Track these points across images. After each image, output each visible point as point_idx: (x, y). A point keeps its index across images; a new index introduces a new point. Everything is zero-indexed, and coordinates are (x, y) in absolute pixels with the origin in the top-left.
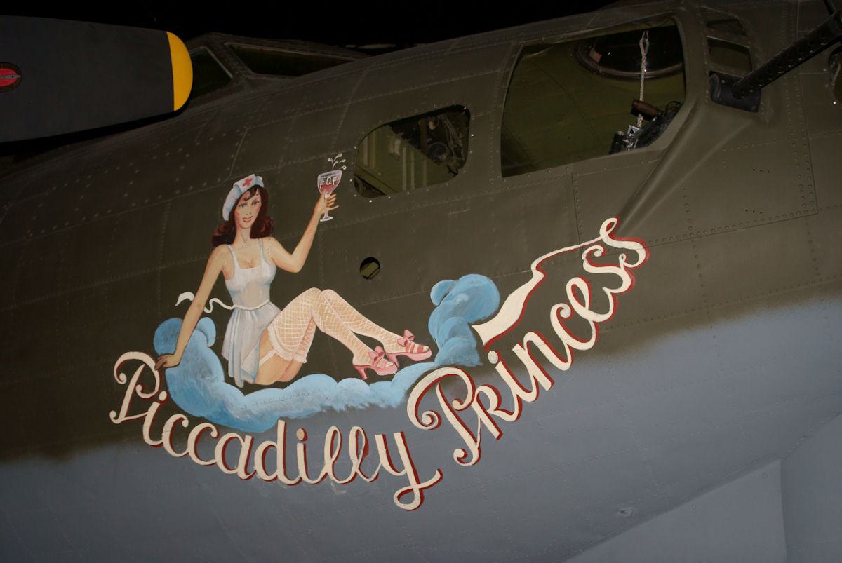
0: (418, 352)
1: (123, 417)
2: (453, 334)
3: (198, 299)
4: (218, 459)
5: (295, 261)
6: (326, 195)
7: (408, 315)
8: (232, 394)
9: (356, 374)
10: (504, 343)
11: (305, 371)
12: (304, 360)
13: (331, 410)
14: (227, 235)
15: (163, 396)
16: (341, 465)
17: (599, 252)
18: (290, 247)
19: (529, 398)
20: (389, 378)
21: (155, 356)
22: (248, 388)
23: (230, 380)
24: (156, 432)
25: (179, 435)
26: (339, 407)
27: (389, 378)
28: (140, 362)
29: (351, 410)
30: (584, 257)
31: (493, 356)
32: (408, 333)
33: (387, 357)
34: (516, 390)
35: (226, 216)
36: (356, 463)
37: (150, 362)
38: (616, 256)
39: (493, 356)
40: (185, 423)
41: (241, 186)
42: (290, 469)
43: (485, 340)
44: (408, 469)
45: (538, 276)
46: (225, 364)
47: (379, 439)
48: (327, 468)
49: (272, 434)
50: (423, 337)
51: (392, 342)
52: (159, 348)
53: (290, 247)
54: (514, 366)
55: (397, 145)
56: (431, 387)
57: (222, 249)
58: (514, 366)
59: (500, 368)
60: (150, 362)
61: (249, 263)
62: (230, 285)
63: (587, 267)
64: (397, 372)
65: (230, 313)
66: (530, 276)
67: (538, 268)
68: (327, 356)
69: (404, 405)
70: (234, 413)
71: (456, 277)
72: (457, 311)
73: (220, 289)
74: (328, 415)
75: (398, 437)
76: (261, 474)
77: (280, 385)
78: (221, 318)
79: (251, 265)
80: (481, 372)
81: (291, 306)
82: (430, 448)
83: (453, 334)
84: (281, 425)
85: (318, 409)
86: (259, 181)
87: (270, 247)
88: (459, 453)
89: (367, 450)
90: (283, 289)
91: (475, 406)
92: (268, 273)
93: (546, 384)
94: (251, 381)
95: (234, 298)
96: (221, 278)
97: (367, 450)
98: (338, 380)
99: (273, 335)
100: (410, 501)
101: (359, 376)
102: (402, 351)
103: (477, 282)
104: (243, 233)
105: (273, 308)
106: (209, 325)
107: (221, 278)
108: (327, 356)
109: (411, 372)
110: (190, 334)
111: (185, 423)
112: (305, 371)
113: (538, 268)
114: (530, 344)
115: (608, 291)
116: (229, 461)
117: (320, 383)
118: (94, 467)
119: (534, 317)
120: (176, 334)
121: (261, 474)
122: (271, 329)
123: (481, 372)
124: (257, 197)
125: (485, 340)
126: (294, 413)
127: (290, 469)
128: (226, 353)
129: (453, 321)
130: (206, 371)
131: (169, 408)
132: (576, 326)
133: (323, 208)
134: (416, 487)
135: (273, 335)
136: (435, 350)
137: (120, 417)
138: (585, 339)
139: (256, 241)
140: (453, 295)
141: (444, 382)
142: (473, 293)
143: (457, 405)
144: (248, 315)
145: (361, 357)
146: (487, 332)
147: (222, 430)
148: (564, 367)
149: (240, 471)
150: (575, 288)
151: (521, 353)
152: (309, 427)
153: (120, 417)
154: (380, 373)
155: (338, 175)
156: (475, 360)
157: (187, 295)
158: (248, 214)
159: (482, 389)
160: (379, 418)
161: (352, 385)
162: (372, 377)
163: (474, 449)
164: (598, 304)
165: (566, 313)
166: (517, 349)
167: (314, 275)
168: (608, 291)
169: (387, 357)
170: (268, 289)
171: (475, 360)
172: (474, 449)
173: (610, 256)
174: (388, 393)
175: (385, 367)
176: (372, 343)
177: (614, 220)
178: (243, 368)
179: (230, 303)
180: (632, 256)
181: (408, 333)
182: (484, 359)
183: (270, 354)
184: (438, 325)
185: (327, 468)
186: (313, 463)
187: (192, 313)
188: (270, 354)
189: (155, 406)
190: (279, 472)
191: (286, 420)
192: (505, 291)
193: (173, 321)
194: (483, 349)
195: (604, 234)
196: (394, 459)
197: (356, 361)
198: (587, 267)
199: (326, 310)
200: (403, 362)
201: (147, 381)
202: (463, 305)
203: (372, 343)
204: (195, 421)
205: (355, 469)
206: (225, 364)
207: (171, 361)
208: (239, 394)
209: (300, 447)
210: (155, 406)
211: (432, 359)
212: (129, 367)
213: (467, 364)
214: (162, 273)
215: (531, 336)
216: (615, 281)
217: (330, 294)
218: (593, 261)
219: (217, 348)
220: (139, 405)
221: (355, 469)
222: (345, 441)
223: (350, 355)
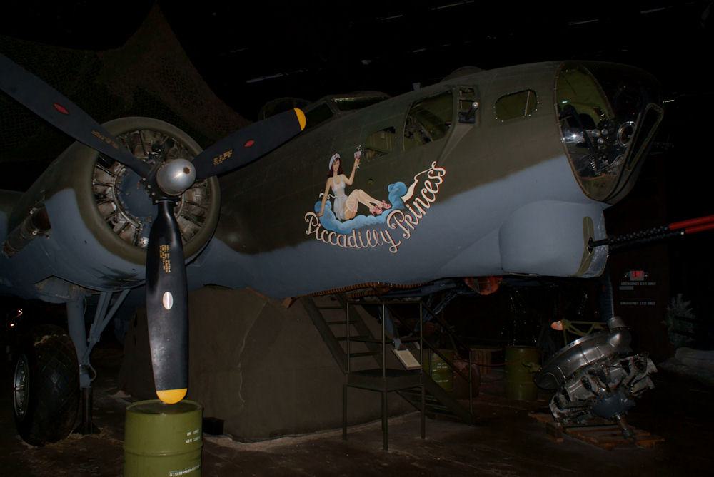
0: (386, 206)
1: (310, 232)
2: (396, 200)
3: (325, 195)
4: (338, 242)
5: (350, 181)
6: (357, 160)
7: (382, 195)
9: (371, 214)
10: (410, 201)
11: (357, 214)
12: (356, 211)
13: (366, 225)
14: (331, 175)
15: (320, 225)
16: (373, 242)
17: (432, 172)
19: (420, 217)
20: (381, 215)
21: (316, 213)
22: (343, 221)
23: (337, 219)
24: (319, 236)
25: (326, 236)
26: (368, 224)
27: (381, 215)
28: (311, 216)
29: (372, 225)
31: (408, 206)
34: (416, 215)
35: (330, 168)
36: (376, 240)
37: (315, 216)
38: (437, 173)
39: (408, 206)
40: (327, 233)
41: (334, 158)
42: (359, 244)
43: (405, 201)
44: (391, 241)
45: (416, 181)
46: (335, 214)
47: (381, 233)
48: (369, 243)
49: (351, 234)
50: (388, 202)
51: (379, 204)
52: (317, 210)
53: (348, 177)
54: (414, 208)
55: (383, 135)
57: (330, 179)
58: (414, 208)
59: (410, 209)
60: (315, 216)
61: (338, 183)
62: (334, 190)
63: (430, 177)
64: (383, 213)
65: (334, 199)
67: (417, 178)
68: (362, 210)
69: (386, 222)
70: (340, 228)
73: (331, 192)
74: (366, 227)
75: (386, 231)
76: (351, 246)
78: (332, 200)
79: (338, 183)
80: (405, 211)
82: (396, 234)
83: (396, 200)
85: (363, 225)
86: (338, 155)
87: (343, 177)
88: (404, 235)
89: (379, 236)
90: (348, 190)
91: (406, 221)
92: (343, 186)
93: (424, 213)
95: (335, 194)
96: (331, 188)
97: (379, 236)
98: (367, 216)
99: (347, 203)
102: (383, 206)
104: (335, 173)
106: (329, 202)
107: (331, 188)
108: (362, 210)
109: (386, 213)
110: (325, 205)
111: (327, 233)
112: (357, 214)
113: (417, 178)
114: (418, 202)
116: (341, 242)
117: (362, 218)
118: (304, 247)
119: (417, 193)
120: (320, 206)
121: (351, 246)
123: (405, 211)
124: (338, 161)
125: (405, 201)
126: (356, 227)
127: (359, 244)
128: (335, 211)
129: (395, 196)
130: (329, 216)
131: (322, 229)
133: (356, 164)
134: (395, 246)
135: (347, 203)
136: (391, 205)
137: (309, 232)
139: (339, 176)
141: (396, 214)
142: (399, 187)
145: (372, 209)
146: (405, 198)
147: (338, 234)
148: (428, 207)
149: (345, 245)
152: (362, 230)
153: (309, 232)
155: (360, 153)
156: (403, 207)
157: (322, 194)
158: (336, 167)
159: (407, 216)
160: (380, 227)
162: (376, 215)
163: (408, 234)
164: (434, 188)
165: (426, 192)
166: (414, 203)
170: (343, 191)
172: (408, 234)
173: (435, 173)
174: (381, 219)
175: (379, 212)
176: (374, 205)
177: (435, 162)
178: (340, 214)
180: (442, 173)
182: (405, 207)
184: (391, 198)
185: (369, 243)
187: (324, 199)
189: (318, 229)
190: (356, 245)
191: (356, 230)
193: (319, 202)
194: (405, 204)
195: (433, 166)
196: (386, 238)
197: (371, 210)
198: (430, 177)
199: (360, 196)
200: (384, 209)
201: (314, 221)
202: (397, 191)
203: (374, 205)
204: (330, 232)
205: (377, 242)
206: (335, 214)
207: (320, 214)
210: (318, 229)
211: (391, 208)
212: (309, 217)
213: (400, 208)
214: (314, 189)
215: (417, 199)
216: (438, 181)
217: (361, 191)
218: (431, 175)
219: (332, 209)
220: (314, 229)
221: (377, 242)
223: (368, 209)
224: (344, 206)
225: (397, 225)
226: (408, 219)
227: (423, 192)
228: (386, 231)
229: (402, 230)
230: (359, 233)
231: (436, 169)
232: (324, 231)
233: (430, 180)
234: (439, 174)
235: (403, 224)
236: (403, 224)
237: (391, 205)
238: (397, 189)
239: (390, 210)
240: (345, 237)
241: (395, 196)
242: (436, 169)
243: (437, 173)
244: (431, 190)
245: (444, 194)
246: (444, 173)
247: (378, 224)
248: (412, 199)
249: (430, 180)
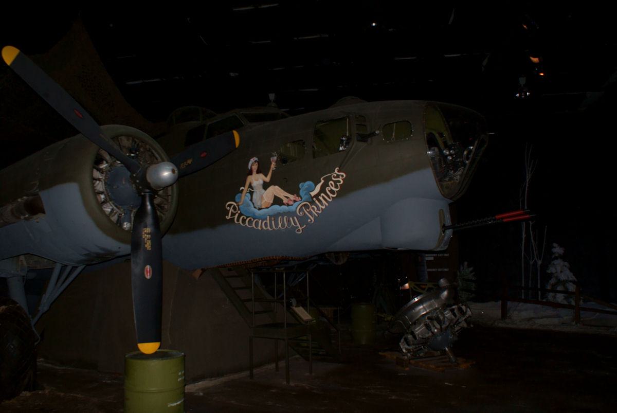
0: (297, 199)
2: (305, 194)
5: (268, 179)
8: (256, 211)
10: (317, 196)
11: (272, 204)
12: (272, 202)
16: (283, 225)
18: (266, 176)
19: (324, 207)
20: (292, 205)
22: (260, 209)
23: (255, 207)
26: (281, 212)
27: (292, 205)
30: (332, 176)
31: (315, 199)
32: (295, 195)
33: (291, 200)
34: (320, 206)
38: (339, 176)
39: (315, 199)
45: (323, 181)
46: (253, 204)
47: (291, 219)
50: (299, 196)
51: (292, 197)
53: (266, 176)
54: (320, 201)
56: (302, 207)
58: (320, 201)
59: (317, 202)
61: (257, 180)
63: (333, 179)
66: (320, 181)
68: (277, 201)
69: (296, 211)
71: (305, 182)
72: (306, 189)
74: (279, 214)
75: (295, 218)
77: (267, 208)
80: (313, 203)
81: (268, 190)
82: (303, 220)
84: (268, 217)
89: (289, 221)
90: (266, 186)
91: (312, 210)
92: (261, 182)
93: (327, 204)
94: (260, 207)
95: (254, 188)
97: (289, 221)
100: (299, 231)
101: (285, 205)
102: (294, 199)
103: (309, 183)
105: (263, 190)
108: (277, 201)
109: (296, 204)
112: (272, 204)
115: (338, 184)
119: (323, 190)
122: (264, 195)
123: (313, 203)
126: (271, 214)
128: (253, 202)
129: (306, 191)
132: (332, 192)
136: (301, 198)
138: (334, 194)
140: (304, 186)
141: (304, 205)
143: (308, 210)
144: (258, 192)
145: (285, 201)
146: (313, 194)
148: (330, 200)
150: (331, 184)
151: (321, 198)
152: (275, 216)
154: (290, 204)
156: (311, 200)
157: (242, 188)
161: (283, 206)
162: (288, 205)
164: (336, 187)
165: (329, 189)
166: (320, 197)
167: (273, 182)
168: (338, 184)
169: (291, 200)
170: (262, 186)
171: (311, 200)
173: (338, 176)
174: (292, 208)
175: (291, 203)
178: (258, 204)
179: (253, 189)
180: (342, 176)
181: (295, 195)
182: (313, 199)
183: (264, 201)
184: (302, 193)
186: (277, 225)
188: (264, 201)
191: (269, 216)
192: (316, 185)
194: (312, 198)
195: (336, 171)
196: (295, 222)
197: (284, 202)
198: (333, 179)
200: (295, 201)
203: (287, 197)
206: (253, 204)
208: (257, 211)
209: (273, 222)
213: (308, 200)
215: (323, 194)
216: (339, 182)
217: (277, 187)
218: (335, 177)
222: (283, 220)
224: (262, 198)
225: (305, 213)
226: (314, 209)
227: (327, 189)
228: (295, 218)
229: (308, 216)
230: (273, 219)
231: (339, 174)
232: (242, 217)
233: (333, 181)
234: (340, 177)
235: (310, 213)
236: (310, 213)
237: (301, 198)
238: (306, 187)
239: (300, 202)
240: (260, 222)
241: (306, 191)
242: (339, 174)
243: (339, 176)
244: (333, 189)
245: (344, 190)
246: (345, 176)
247: (289, 212)
248: (319, 194)
249: (333, 181)
